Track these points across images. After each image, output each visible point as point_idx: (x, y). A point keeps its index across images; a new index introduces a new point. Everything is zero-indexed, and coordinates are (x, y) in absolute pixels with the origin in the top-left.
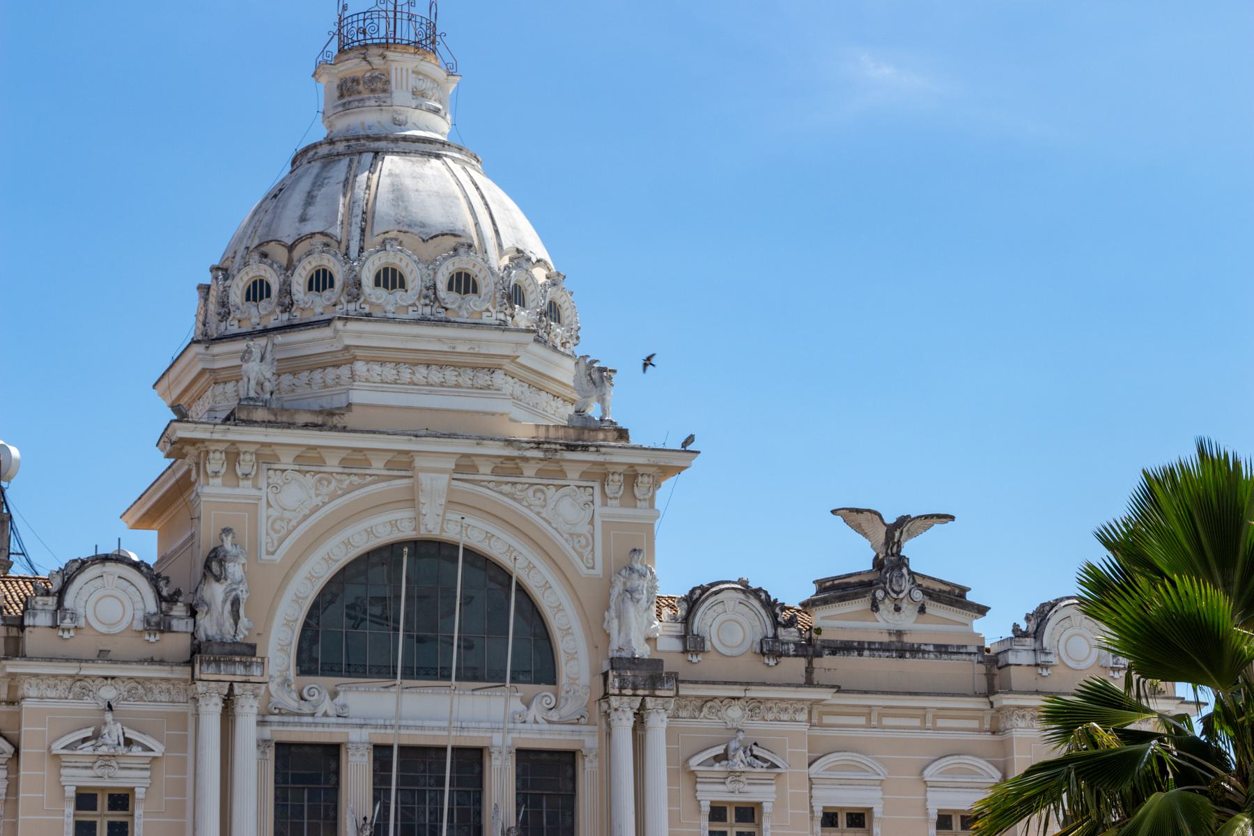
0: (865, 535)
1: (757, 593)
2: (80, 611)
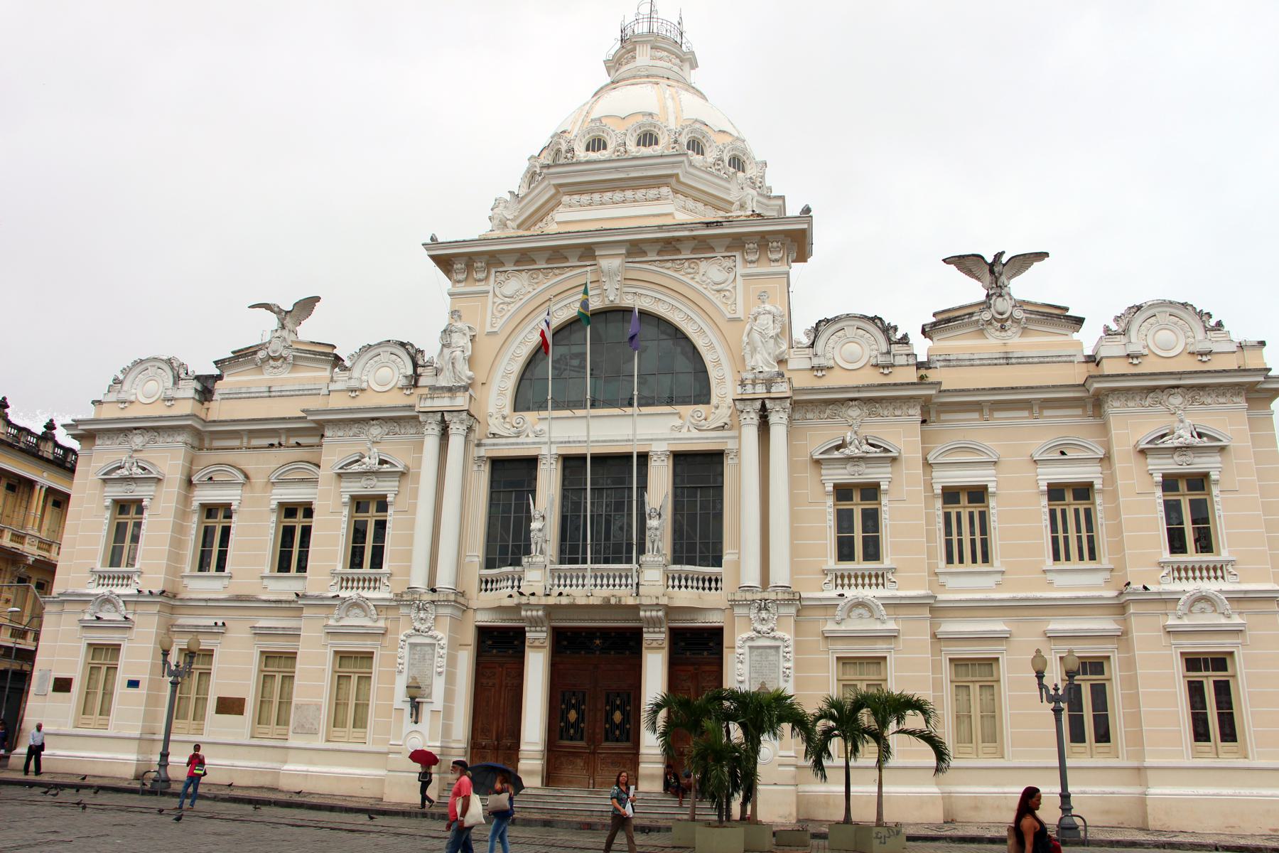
0: (978, 279)
1: (874, 319)
2: (364, 378)
